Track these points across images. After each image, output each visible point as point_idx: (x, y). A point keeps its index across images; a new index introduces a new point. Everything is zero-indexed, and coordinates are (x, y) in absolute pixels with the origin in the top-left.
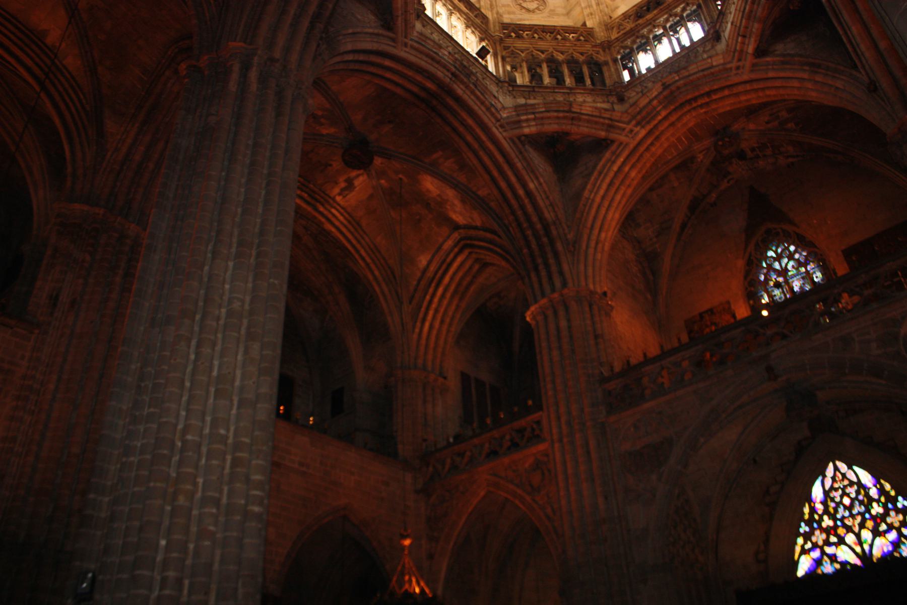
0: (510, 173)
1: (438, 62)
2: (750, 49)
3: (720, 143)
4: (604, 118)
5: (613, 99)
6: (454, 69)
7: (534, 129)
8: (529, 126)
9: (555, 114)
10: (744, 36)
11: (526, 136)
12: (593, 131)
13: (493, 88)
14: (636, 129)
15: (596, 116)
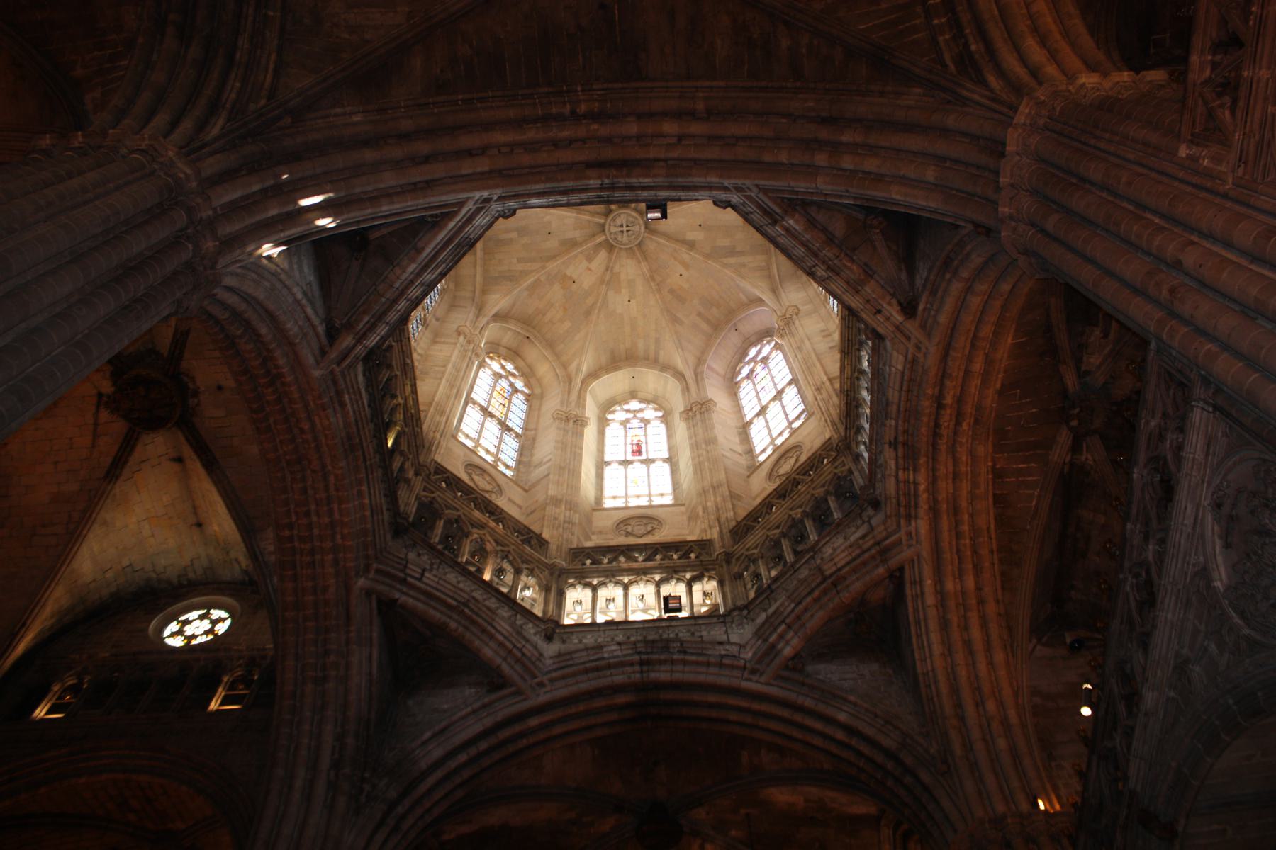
0: (809, 722)
1: (609, 667)
2: (899, 318)
3: (1074, 423)
4: (869, 549)
5: (870, 512)
6: (636, 658)
7: (795, 641)
8: (788, 643)
9: (809, 599)
10: (879, 312)
11: (793, 658)
12: (868, 578)
13: (718, 633)
14: (912, 528)
15: (859, 556)
